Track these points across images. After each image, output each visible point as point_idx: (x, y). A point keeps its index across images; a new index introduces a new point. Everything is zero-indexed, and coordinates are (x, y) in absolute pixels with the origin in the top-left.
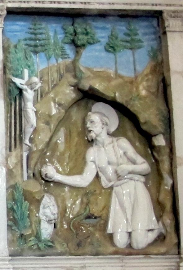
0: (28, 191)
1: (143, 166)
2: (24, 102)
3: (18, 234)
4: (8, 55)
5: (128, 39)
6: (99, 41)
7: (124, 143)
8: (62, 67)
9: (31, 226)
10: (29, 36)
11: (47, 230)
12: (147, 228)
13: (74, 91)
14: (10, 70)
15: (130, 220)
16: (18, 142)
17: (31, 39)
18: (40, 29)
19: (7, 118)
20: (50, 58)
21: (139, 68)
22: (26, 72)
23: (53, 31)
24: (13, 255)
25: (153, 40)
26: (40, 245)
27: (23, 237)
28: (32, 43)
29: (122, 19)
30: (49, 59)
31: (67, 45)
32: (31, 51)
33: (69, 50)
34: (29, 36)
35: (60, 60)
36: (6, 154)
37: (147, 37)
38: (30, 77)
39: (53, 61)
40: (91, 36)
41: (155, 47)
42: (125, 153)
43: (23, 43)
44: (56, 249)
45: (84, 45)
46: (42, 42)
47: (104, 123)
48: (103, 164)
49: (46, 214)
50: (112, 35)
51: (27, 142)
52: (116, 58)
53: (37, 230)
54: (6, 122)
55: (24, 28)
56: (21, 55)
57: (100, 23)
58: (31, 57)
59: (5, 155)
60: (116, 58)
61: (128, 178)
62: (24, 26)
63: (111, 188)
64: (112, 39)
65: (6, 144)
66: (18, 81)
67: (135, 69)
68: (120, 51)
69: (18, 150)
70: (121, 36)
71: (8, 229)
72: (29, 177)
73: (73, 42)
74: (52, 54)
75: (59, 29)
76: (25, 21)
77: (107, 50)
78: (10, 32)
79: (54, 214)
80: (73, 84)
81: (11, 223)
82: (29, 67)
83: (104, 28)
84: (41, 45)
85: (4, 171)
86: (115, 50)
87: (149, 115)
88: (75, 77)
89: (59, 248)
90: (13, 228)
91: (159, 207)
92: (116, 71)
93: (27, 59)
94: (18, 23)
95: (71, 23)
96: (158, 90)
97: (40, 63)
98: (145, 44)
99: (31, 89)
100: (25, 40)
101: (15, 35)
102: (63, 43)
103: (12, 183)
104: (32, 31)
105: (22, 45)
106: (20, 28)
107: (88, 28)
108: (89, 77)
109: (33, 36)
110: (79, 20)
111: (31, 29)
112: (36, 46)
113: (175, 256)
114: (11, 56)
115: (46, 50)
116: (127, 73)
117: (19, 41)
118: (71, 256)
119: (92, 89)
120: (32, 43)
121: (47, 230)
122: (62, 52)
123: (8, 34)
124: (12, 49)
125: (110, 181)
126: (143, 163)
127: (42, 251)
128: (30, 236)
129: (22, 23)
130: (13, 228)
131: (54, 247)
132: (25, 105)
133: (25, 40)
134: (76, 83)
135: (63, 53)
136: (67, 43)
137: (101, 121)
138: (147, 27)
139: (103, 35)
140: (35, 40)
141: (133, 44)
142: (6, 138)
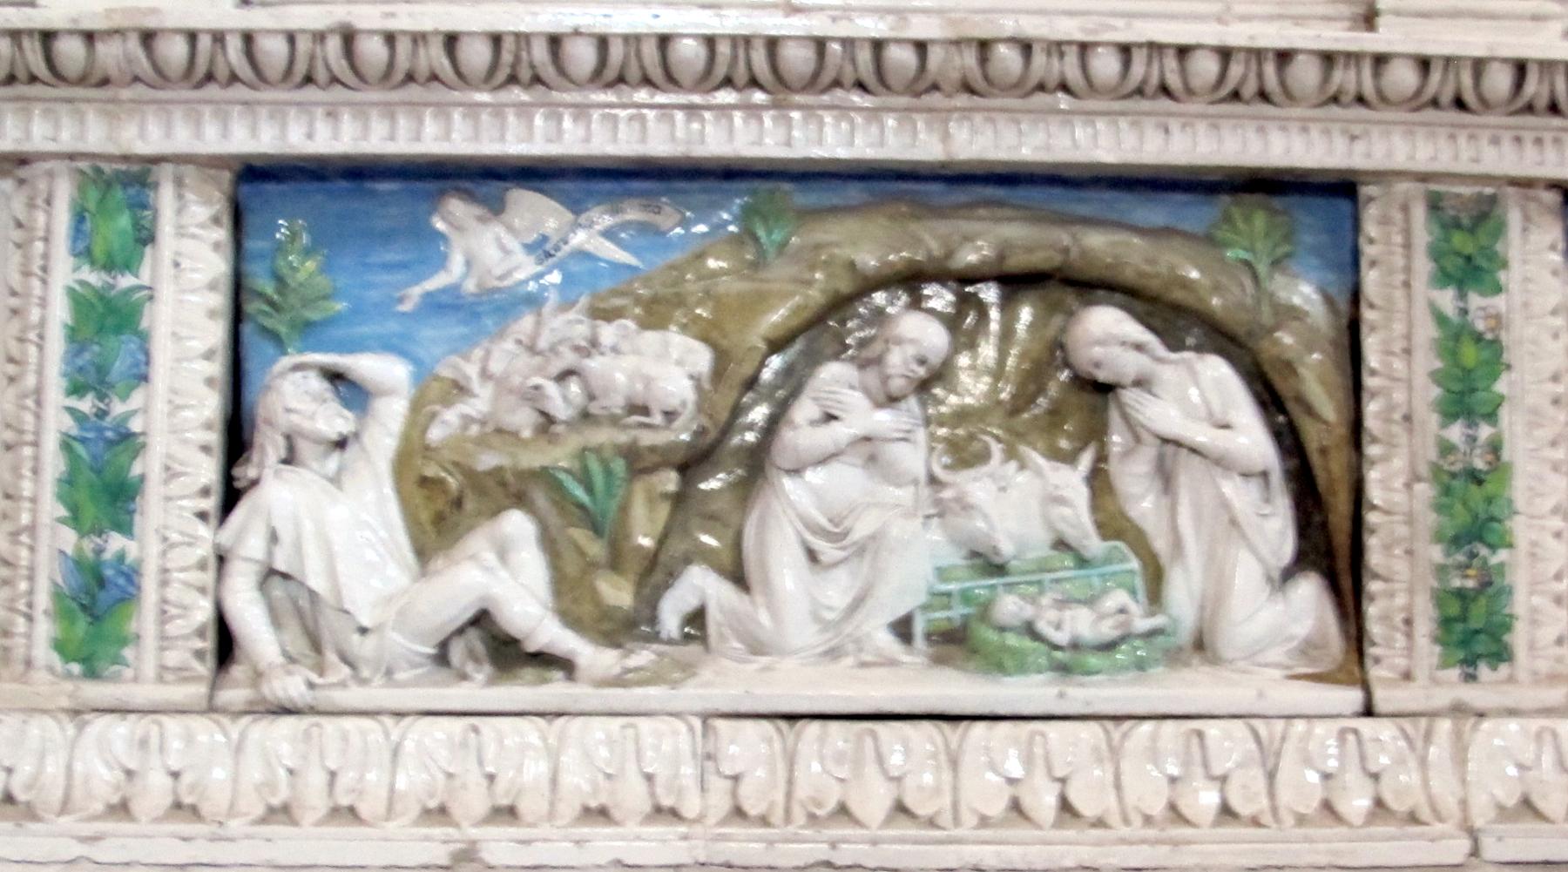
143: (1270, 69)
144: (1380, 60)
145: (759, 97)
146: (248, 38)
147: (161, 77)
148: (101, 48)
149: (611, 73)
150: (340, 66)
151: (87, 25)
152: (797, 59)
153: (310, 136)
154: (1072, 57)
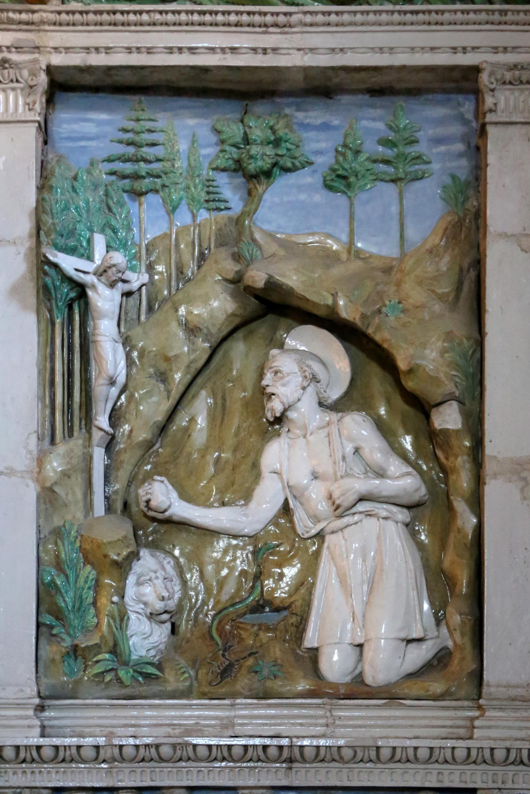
1: (403, 480)
4: (46, 196)
5: (389, 153)
6: (311, 164)
7: (358, 428)
8: (206, 233)
11: (145, 639)
12: (403, 635)
13: (234, 295)
15: (359, 616)
18: (150, 131)
20: (175, 209)
21: (413, 233)
22: (99, 242)
23: (188, 136)
25: (460, 155)
26: (122, 673)
27: (79, 652)
29: (378, 101)
30: (172, 209)
31: (224, 175)
32: (125, 191)
33: (230, 190)
35: (203, 215)
37: (442, 148)
39: (183, 217)
40: (288, 150)
41: (463, 175)
42: (357, 450)
44: (166, 681)
45: (268, 174)
46: (156, 167)
47: (307, 374)
48: (300, 476)
49: (145, 599)
50: (345, 146)
52: (351, 205)
53: (114, 635)
55: (108, 129)
56: (94, 199)
57: (315, 114)
59: (35, 453)
60: (351, 205)
61: (360, 513)
63: (320, 536)
64: (344, 155)
66: (68, 263)
67: (402, 236)
68: (362, 188)
70: (373, 148)
73: (238, 168)
74: (181, 199)
75: (205, 134)
76: (109, 110)
77: (329, 187)
79: (163, 597)
80: (230, 276)
83: (326, 127)
84: (150, 175)
85: (30, 492)
86: (349, 186)
87: (426, 355)
88: (237, 257)
89: (173, 680)
90: (55, 632)
91: (437, 582)
92: (351, 242)
93: (110, 209)
95: (238, 116)
96: (459, 289)
97: (150, 220)
98: (435, 166)
100: (109, 160)
101: (85, 147)
102: (213, 169)
105: (101, 173)
106: (93, 130)
107: (280, 126)
108: (273, 255)
109: (131, 150)
110: (259, 107)
112: (136, 177)
113: (466, 703)
115: (164, 186)
116: (376, 245)
118: (200, 698)
119: (272, 285)
120: (128, 168)
121: (145, 639)
122: (208, 193)
125: (316, 519)
126: (408, 474)
127: (127, 686)
128: (97, 648)
129: (104, 116)
130: (55, 632)
131: (161, 677)
133: (109, 160)
134: (237, 272)
135: (212, 196)
136: (224, 170)
137: (303, 367)
138: (441, 121)
139: (323, 145)
140: (137, 160)
141: (400, 167)
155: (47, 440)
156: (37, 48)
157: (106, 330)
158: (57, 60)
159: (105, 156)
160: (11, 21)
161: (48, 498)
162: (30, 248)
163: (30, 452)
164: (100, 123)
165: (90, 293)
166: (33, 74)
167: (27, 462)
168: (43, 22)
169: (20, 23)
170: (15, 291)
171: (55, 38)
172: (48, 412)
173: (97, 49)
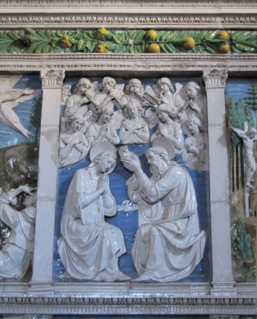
0: (250, 225)
2: (245, 149)
3: (242, 263)
4: (230, 110)
9: (253, 256)
10: (248, 96)
14: (231, 123)
16: (240, 184)
17: (250, 98)
19: (230, 162)
22: (246, 125)
24: (238, 281)
27: (247, 265)
28: (252, 101)
32: (251, 108)
34: (248, 96)
36: (230, 193)
38: (249, 129)
43: (243, 101)
51: (248, 184)
54: (229, 166)
56: (241, 111)
58: (250, 113)
59: (228, 194)
62: (244, 87)
65: (230, 185)
66: (239, 131)
69: (241, 190)
71: (232, 259)
72: (251, 214)
78: (232, 92)
81: (235, 253)
82: (249, 121)
85: (228, 208)
93: (247, 114)
94: (239, 85)
99: (251, 138)
100: (245, 99)
101: (237, 95)
103: (235, 219)
104: (251, 91)
106: (241, 89)
109: (252, 96)
111: (250, 90)
114: (233, 110)
117: (240, 100)
120: (252, 101)
123: (230, 95)
124: (233, 106)
129: (243, 85)
132: (246, 152)
133: (245, 99)
142: (230, 178)
143: (194, 301)
144: (210, 299)
145: (125, 306)
146: (57, 299)
147: (44, 304)
148: (37, 300)
149: (105, 303)
150: (68, 302)
151: (35, 297)
152: (130, 301)
153: (64, 311)
154: (167, 301)
155: (232, 190)
156: (224, 66)
157: (250, 153)
158: (231, 69)
159: (244, 97)
160: (216, 59)
161: (233, 210)
162: (224, 127)
163: (227, 194)
164: (241, 87)
165: (245, 141)
166: (224, 73)
167: (226, 197)
168: (227, 59)
169: (219, 59)
170: (220, 140)
171: (230, 63)
172: (232, 180)
173: (243, 67)
